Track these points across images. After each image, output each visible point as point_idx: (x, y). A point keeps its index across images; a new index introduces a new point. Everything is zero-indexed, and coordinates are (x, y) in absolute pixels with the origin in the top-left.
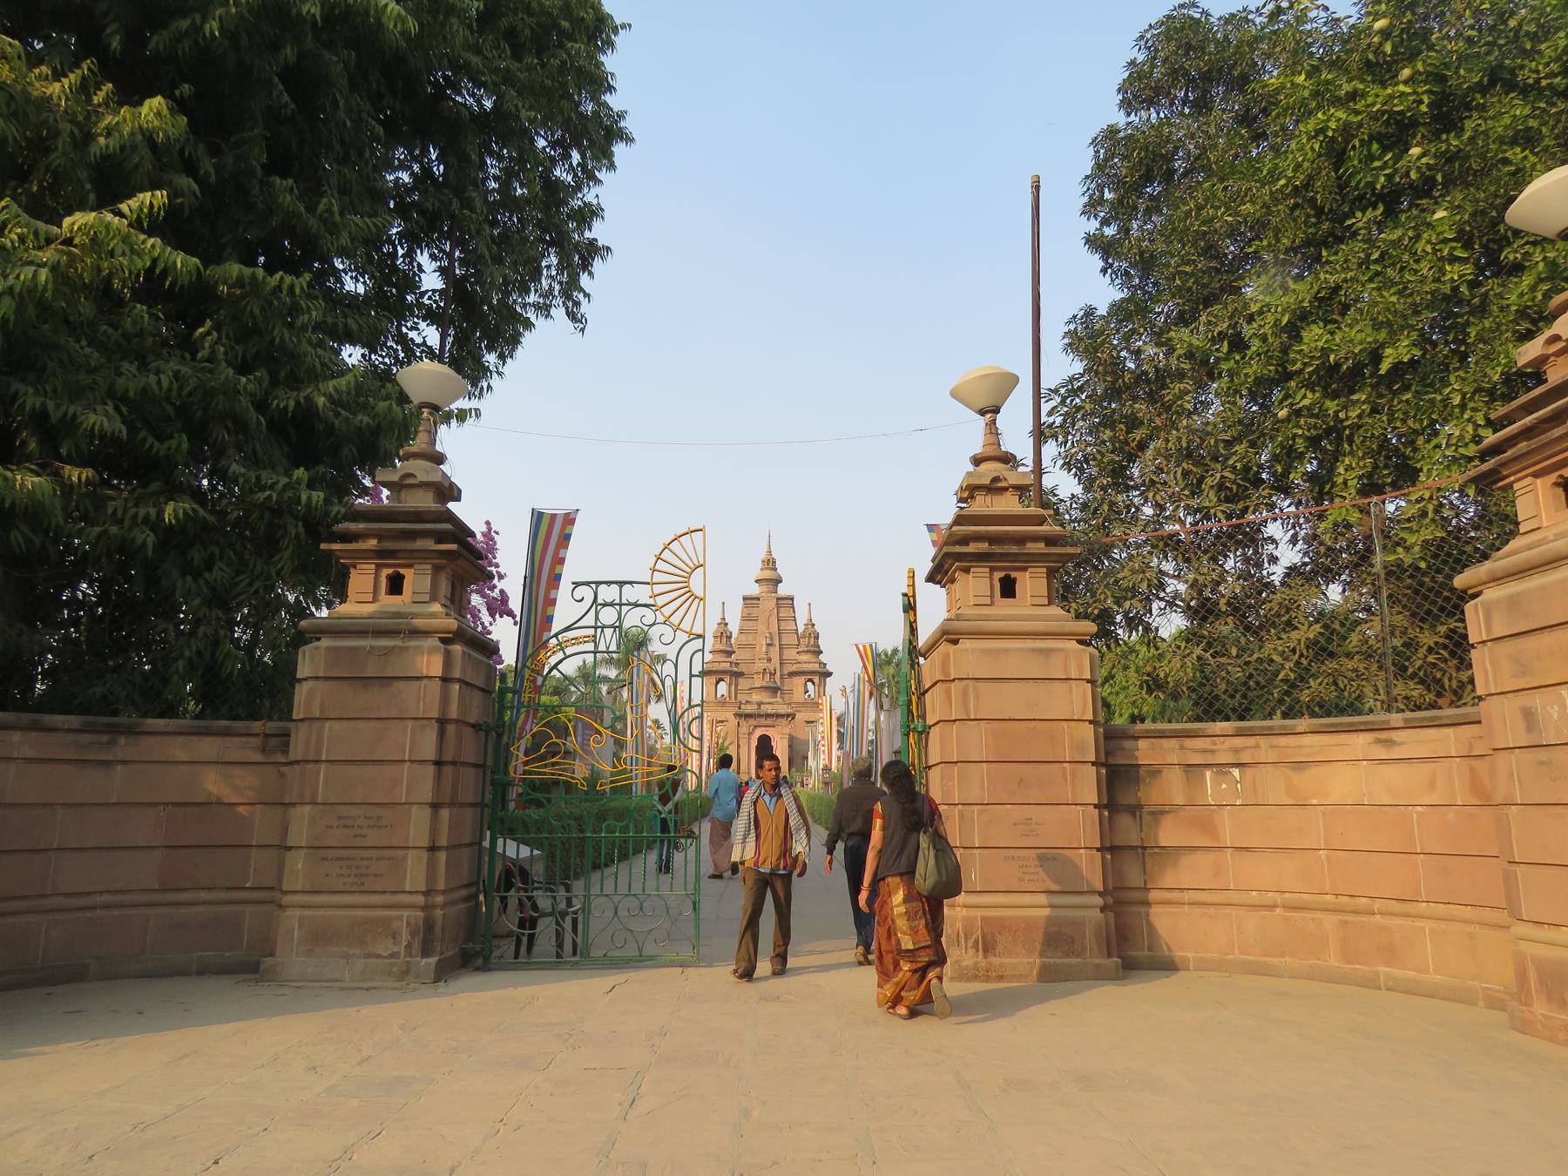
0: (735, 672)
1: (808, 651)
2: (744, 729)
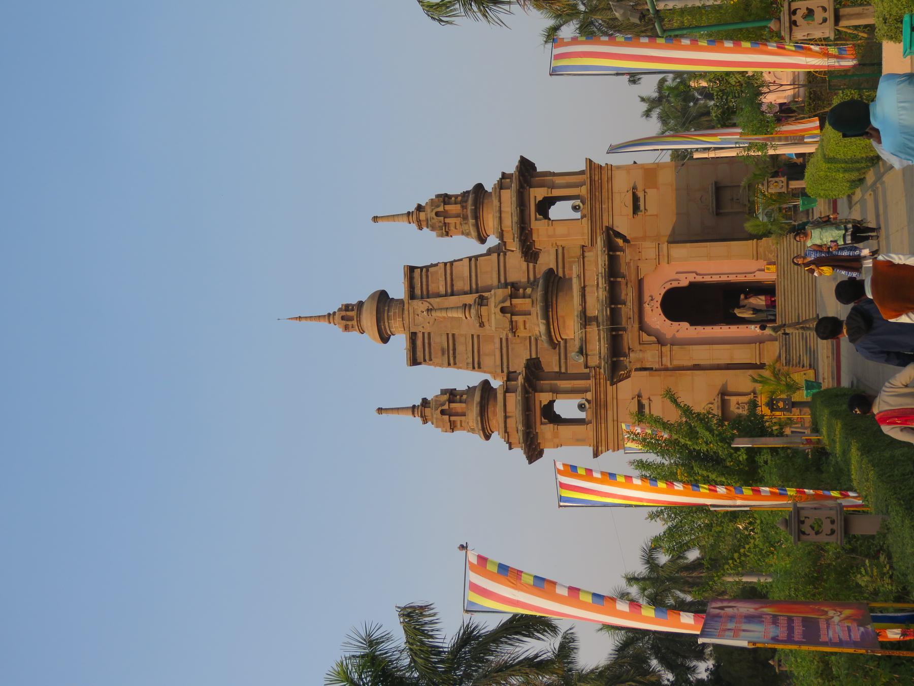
0: (527, 379)
1: (476, 217)
2: (650, 356)
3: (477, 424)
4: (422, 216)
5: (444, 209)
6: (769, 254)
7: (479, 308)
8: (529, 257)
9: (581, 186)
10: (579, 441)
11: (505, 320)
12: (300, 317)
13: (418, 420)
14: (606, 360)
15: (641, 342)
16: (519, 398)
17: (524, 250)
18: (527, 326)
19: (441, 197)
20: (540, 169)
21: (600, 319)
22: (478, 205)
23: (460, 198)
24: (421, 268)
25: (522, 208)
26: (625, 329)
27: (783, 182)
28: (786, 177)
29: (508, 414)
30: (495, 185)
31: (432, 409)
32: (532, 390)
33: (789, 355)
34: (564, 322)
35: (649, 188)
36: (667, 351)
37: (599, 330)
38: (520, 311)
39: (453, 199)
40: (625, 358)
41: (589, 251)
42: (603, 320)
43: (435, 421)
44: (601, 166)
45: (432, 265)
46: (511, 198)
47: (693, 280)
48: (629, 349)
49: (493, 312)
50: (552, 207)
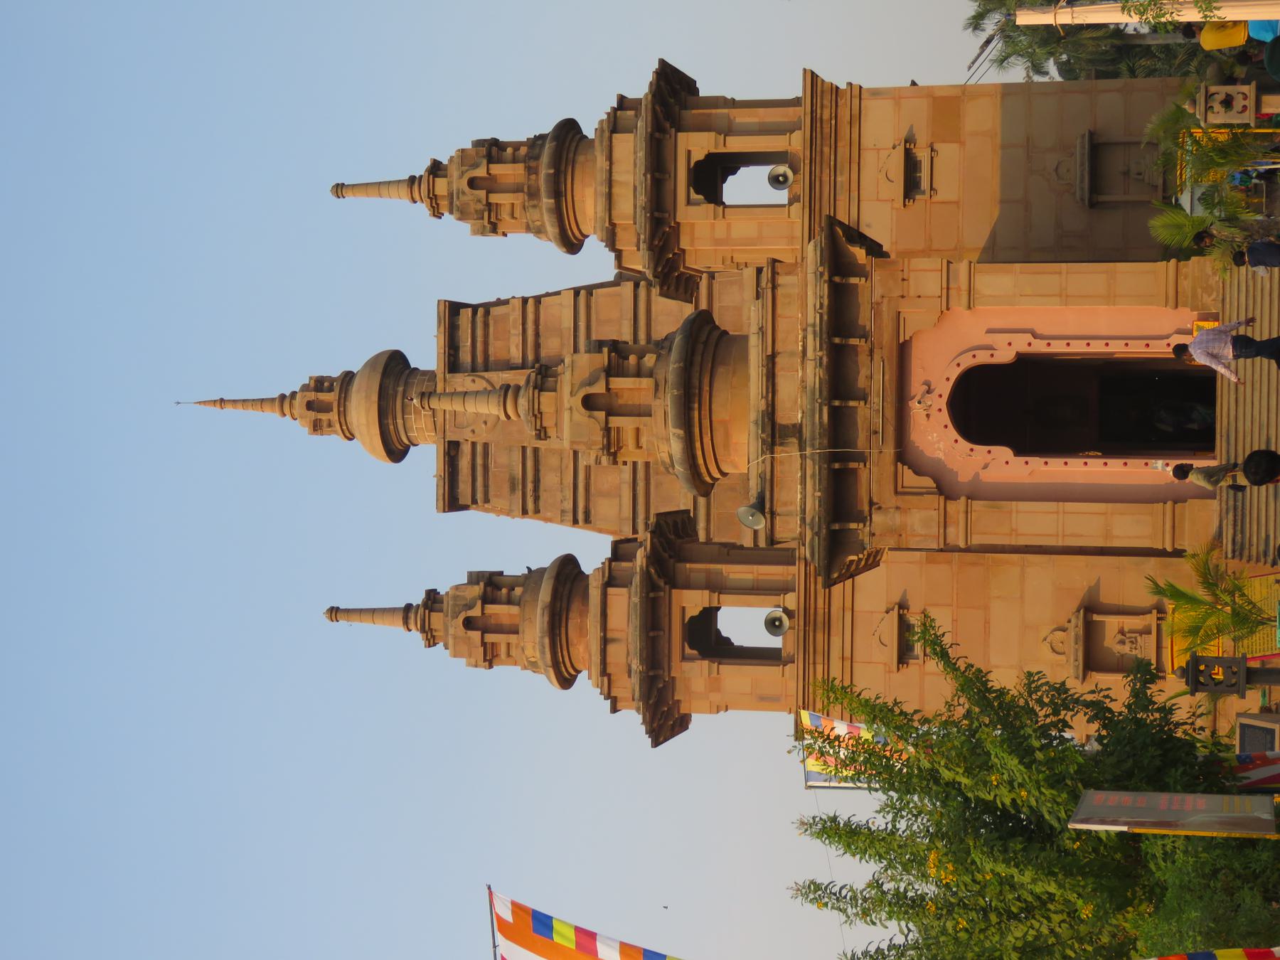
0: (655, 558)
1: (558, 193)
3: (543, 653)
4: (441, 186)
5: (488, 173)
6: (1205, 296)
7: (536, 395)
8: (672, 288)
9: (792, 132)
10: (765, 701)
11: (592, 425)
12: (222, 400)
13: (416, 637)
14: (816, 529)
15: (900, 489)
16: (636, 600)
17: (660, 270)
18: (643, 440)
19: (483, 147)
20: (705, 91)
21: (807, 433)
22: (563, 168)
23: (523, 150)
24: (475, 308)
25: (657, 175)
26: (862, 458)
27: (1245, 97)
28: (1254, 84)
29: (609, 635)
30: (601, 122)
31: (447, 616)
32: (666, 583)
33: (1243, 532)
34: (727, 435)
35: (944, 141)
36: (958, 512)
37: (803, 457)
38: (626, 405)
39: (509, 150)
40: (861, 525)
41: (788, 273)
42: (813, 432)
43: (451, 642)
44: (837, 88)
45: (500, 303)
46: (635, 153)
47: (1024, 349)
48: (871, 503)
49: (567, 405)
50: (730, 178)
